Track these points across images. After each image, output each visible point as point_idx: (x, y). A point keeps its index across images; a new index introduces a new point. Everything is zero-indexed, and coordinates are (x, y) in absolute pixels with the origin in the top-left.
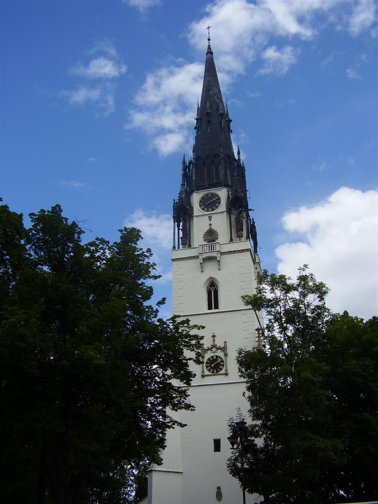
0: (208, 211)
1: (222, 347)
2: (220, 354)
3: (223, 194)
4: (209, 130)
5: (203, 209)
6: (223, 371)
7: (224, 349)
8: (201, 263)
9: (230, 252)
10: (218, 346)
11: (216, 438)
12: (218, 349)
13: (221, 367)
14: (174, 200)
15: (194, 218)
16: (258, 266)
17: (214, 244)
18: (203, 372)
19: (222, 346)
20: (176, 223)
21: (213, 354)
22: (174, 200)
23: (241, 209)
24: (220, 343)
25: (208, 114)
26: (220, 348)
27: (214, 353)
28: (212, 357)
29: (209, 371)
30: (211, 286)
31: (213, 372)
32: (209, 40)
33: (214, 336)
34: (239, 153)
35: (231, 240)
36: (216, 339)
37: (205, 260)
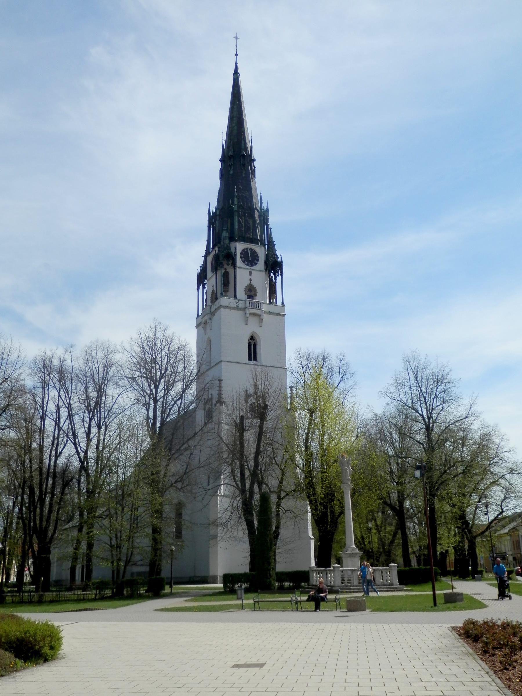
0: (247, 265)
3: (261, 252)
5: (244, 262)
9: (270, 313)
37: (250, 314)
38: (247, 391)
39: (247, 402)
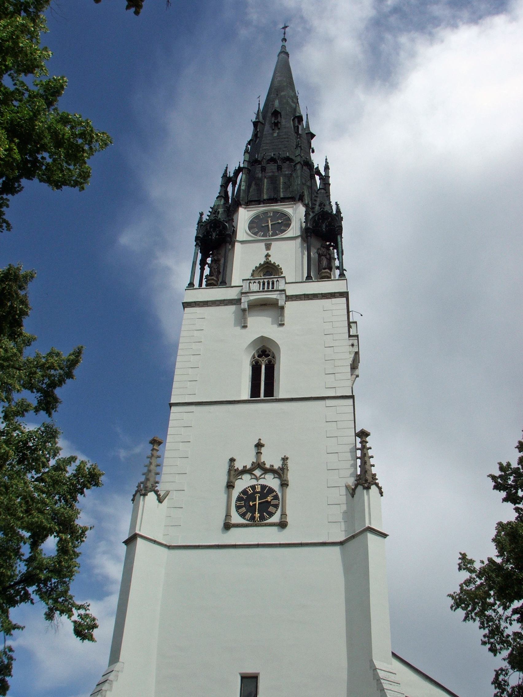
1: (276, 467)
2: (272, 482)
3: (297, 213)
4: (275, 135)
5: (255, 234)
6: (275, 519)
7: (280, 473)
8: (244, 310)
10: (268, 466)
11: (250, 670)
12: (266, 471)
13: (271, 509)
14: (201, 214)
15: (237, 245)
16: (355, 342)
17: (275, 280)
18: (228, 516)
19: (277, 465)
20: (200, 256)
21: (254, 482)
22: (201, 214)
23: (328, 243)
24: (271, 459)
25: (276, 114)
26: (271, 470)
27: (257, 479)
28: (253, 487)
29: (243, 515)
30: (259, 356)
31: (253, 518)
32: (284, 40)
33: (259, 445)
34: (327, 168)
35: (309, 277)
36: (263, 450)
38: (232, 460)
39: (230, 486)
